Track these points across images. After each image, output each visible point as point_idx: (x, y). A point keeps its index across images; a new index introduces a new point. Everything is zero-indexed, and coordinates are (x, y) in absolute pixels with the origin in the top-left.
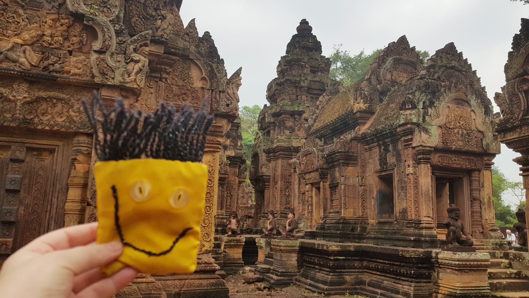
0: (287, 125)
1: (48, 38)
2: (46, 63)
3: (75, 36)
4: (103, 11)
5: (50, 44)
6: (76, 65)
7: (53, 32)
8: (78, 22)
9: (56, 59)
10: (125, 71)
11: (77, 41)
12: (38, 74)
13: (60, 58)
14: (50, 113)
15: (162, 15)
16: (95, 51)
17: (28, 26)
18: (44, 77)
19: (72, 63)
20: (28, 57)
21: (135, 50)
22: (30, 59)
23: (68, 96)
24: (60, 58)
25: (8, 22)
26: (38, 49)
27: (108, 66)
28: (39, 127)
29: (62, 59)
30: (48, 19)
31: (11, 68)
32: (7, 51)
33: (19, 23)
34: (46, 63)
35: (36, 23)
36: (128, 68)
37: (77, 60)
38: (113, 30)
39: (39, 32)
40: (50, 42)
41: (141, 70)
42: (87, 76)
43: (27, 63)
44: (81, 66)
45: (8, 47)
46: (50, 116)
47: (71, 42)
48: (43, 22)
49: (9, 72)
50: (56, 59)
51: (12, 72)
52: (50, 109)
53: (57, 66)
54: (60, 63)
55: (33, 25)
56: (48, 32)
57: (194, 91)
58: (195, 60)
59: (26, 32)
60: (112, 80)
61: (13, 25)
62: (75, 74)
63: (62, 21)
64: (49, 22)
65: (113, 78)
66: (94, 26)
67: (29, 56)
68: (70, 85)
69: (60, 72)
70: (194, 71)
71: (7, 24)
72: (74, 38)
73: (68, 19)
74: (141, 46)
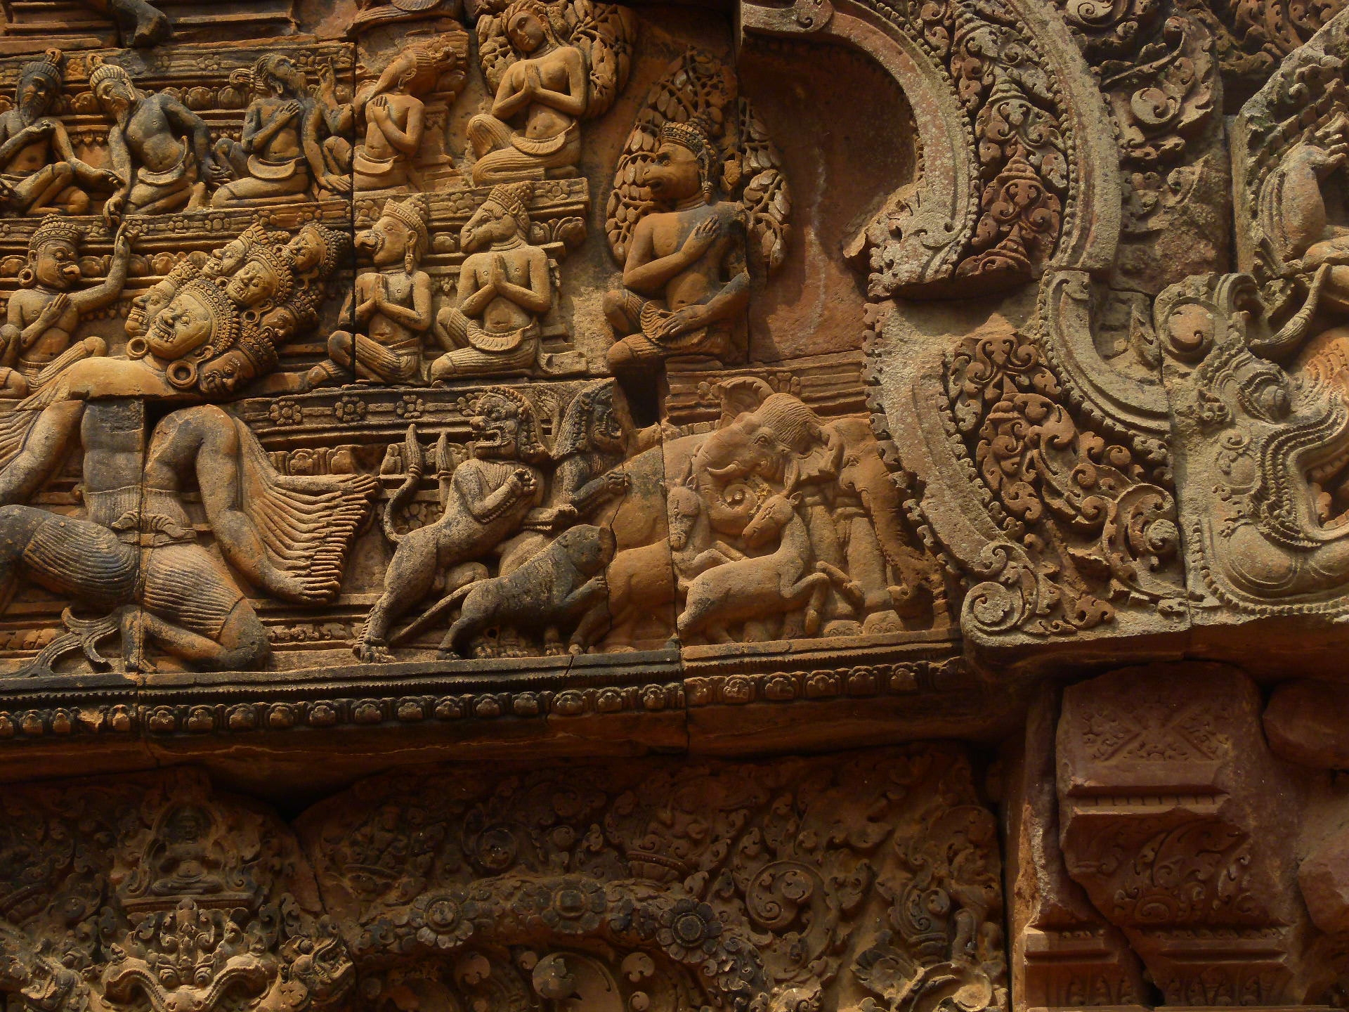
1: (398, 281)
2: (417, 542)
3: (667, 196)
5: (429, 339)
6: (723, 509)
7: (440, 210)
8: (673, 55)
9: (503, 477)
10: (1277, 444)
11: (691, 241)
16: (918, 299)
17: (194, 207)
18: (409, 707)
19: (678, 492)
20: (226, 521)
22: (250, 537)
24: (547, 466)
26: (314, 422)
27: (1083, 421)
29: (568, 471)
30: (367, 91)
34: (417, 542)
35: (261, 151)
36: (1303, 410)
38: (1056, 25)
40: (420, 311)
42: (860, 610)
43: (224, 590)
45: (25, 461)
47: (632, 271)
48: (323, 132)
49: (60, 718)
50: (502, 479)
51: (93, 717)
54: (562, 522)
59: (182, 266)
60: (1163, 586)
62: (727, 615)
63: (518, 69)
64: (392, 110)
65: (1170, 558)
67: (237, 504)
68: (680, 756)
72: (663, 224)
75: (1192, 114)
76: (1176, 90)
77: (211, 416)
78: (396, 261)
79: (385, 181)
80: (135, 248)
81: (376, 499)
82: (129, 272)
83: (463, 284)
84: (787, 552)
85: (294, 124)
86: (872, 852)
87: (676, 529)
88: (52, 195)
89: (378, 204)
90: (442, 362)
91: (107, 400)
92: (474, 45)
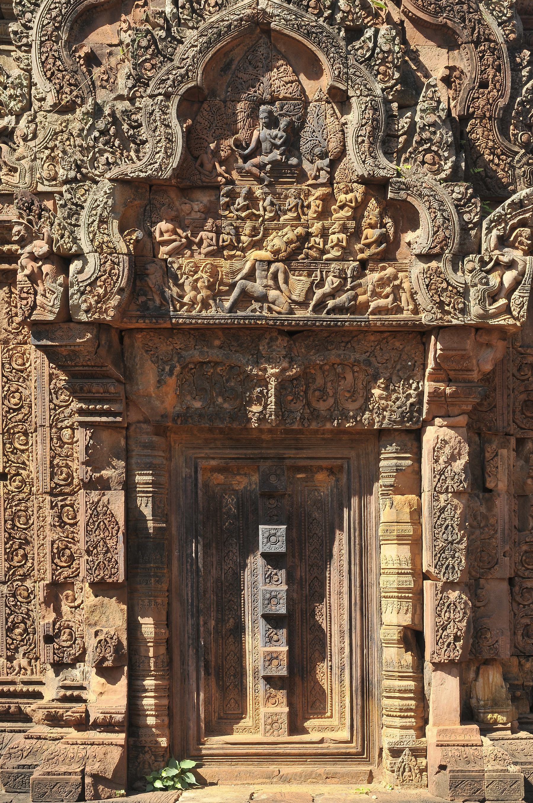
1: (317, 240)
3: (372, 226)
6: (378, 290)
11: (375, 237)
13: (345, 279)
14: (331, 394)
25: (239, 218)
28: (314, 426)
30: (311, 199)
33: (259, 216)
35: (290, 210)
37: (381, 279)
39: (300, 230)
46: (331, 401)
52: (329, 384)
55: (286, 217)
61: (249, 224)
62: (378, 311)
75: (475, 220)
76: (473, 214)
77: (280, 265)
78: (317, 236)
79: (314, 218)
80: (265, 229)
81: (312, 283)
82: (264, 234)
83: (330, 241)
85: (296, 205)
86: (402, 350)
87: (369, 293)
88: (248, 217)
89: (313, 224)
90: (325, 257)
91: (261, 261)
92: (333, 190)
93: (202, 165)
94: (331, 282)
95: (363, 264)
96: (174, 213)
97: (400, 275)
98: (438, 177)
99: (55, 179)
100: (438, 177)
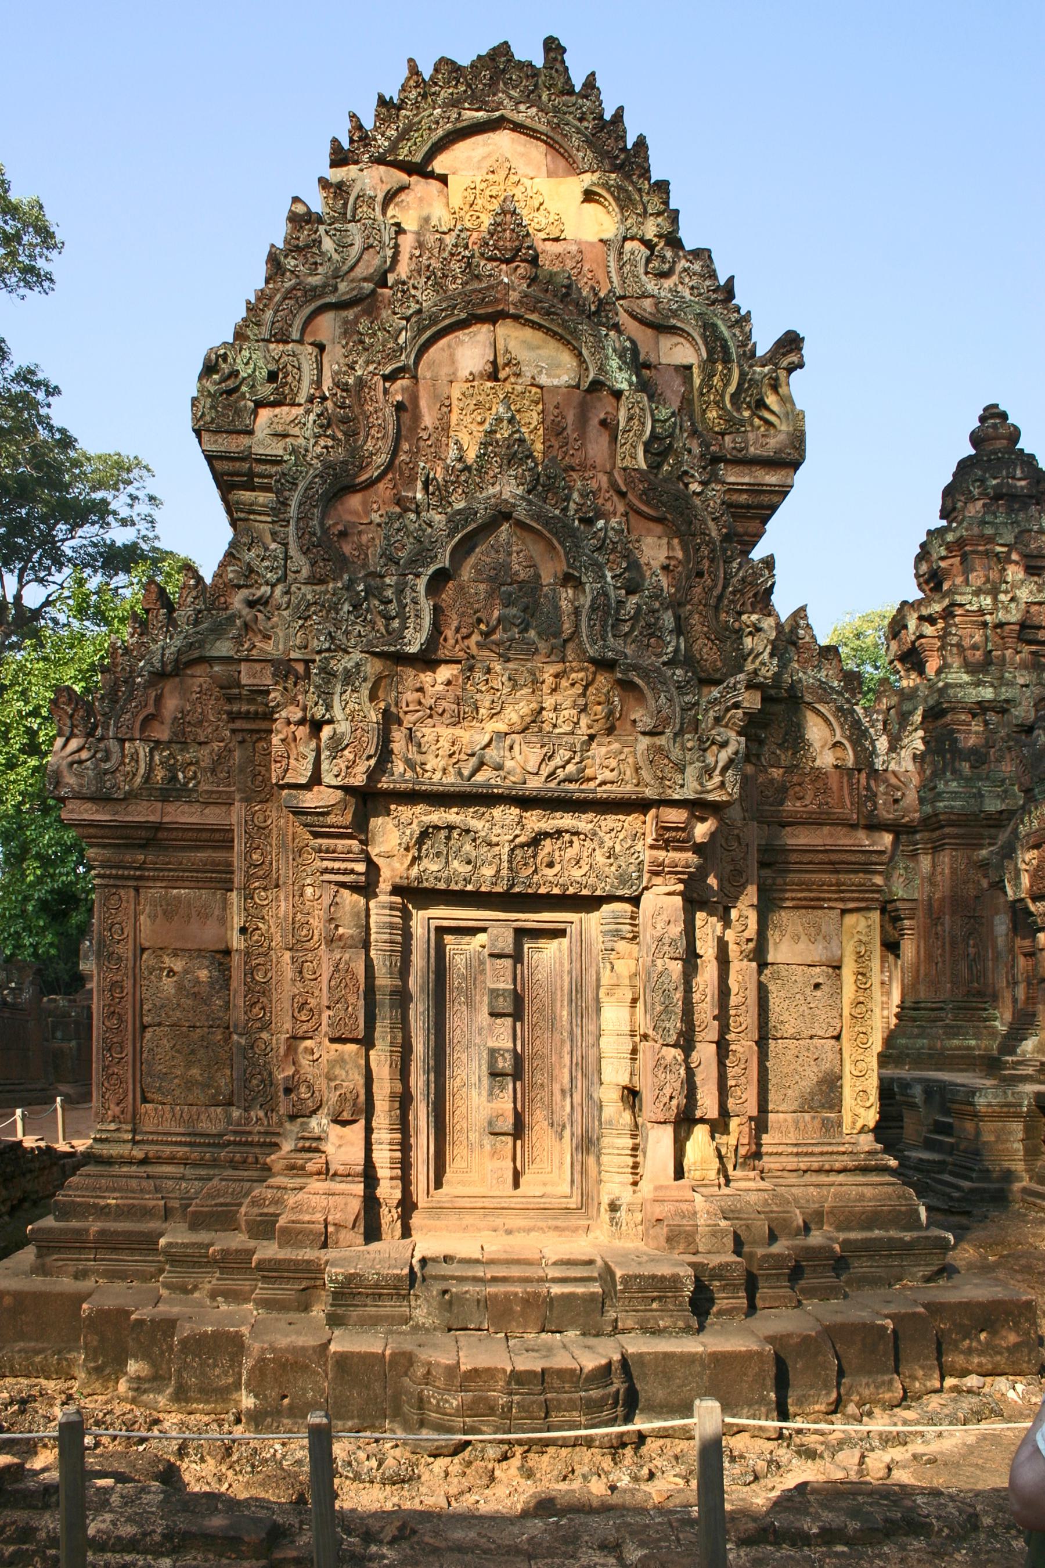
0: (961, 745)
2: (552, 764)
3: (599, 704)
4: (648, 645)
12: (540, 790)
15: (754, 625)
16: (644, 733)
20: (518, 757)
21: (717, 720)
23: (590, 826)
25: (479, 691)
26: (534, 739)
27: (671, 761)
30: (546, 676)
31: (493, 782)
32: (483, 749)
34: (552, 764)
37: (608, 752)
39: (534, 706)
41: (731, 761)
43: (519, 770)
44: (613, 763)
47: (592, 718)
50: (568, 754)
53: (571, 768)
55: (523, 692)
56: (549, 702)
57: (818, 775)
58: (817, 706)
62: (603, 783)
63: (574, 675)
64: (550, 680)
66: (637, 680)
69: (576, 781)
70: (815, 729)
71: (478, 696)
72: (600, 708)
73: (582, 670)
74: (728, 710)
84: (615, 773)
90: (557, 731)
93: (445, 640)
94: (563, 754)
95: (592, 737)
96: (418, 685)
97: (626, 750)
98: (661, 660)
99: (306, 647)
100: (661, 660)
